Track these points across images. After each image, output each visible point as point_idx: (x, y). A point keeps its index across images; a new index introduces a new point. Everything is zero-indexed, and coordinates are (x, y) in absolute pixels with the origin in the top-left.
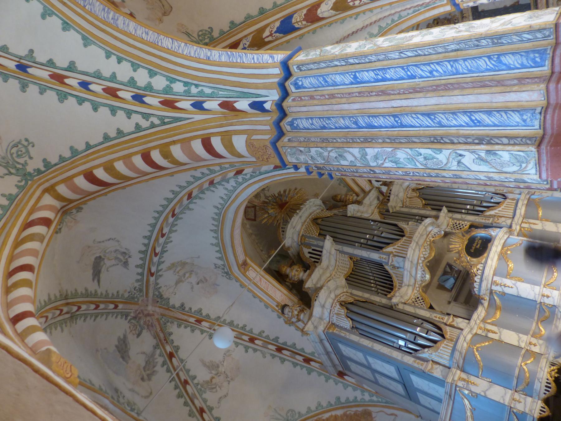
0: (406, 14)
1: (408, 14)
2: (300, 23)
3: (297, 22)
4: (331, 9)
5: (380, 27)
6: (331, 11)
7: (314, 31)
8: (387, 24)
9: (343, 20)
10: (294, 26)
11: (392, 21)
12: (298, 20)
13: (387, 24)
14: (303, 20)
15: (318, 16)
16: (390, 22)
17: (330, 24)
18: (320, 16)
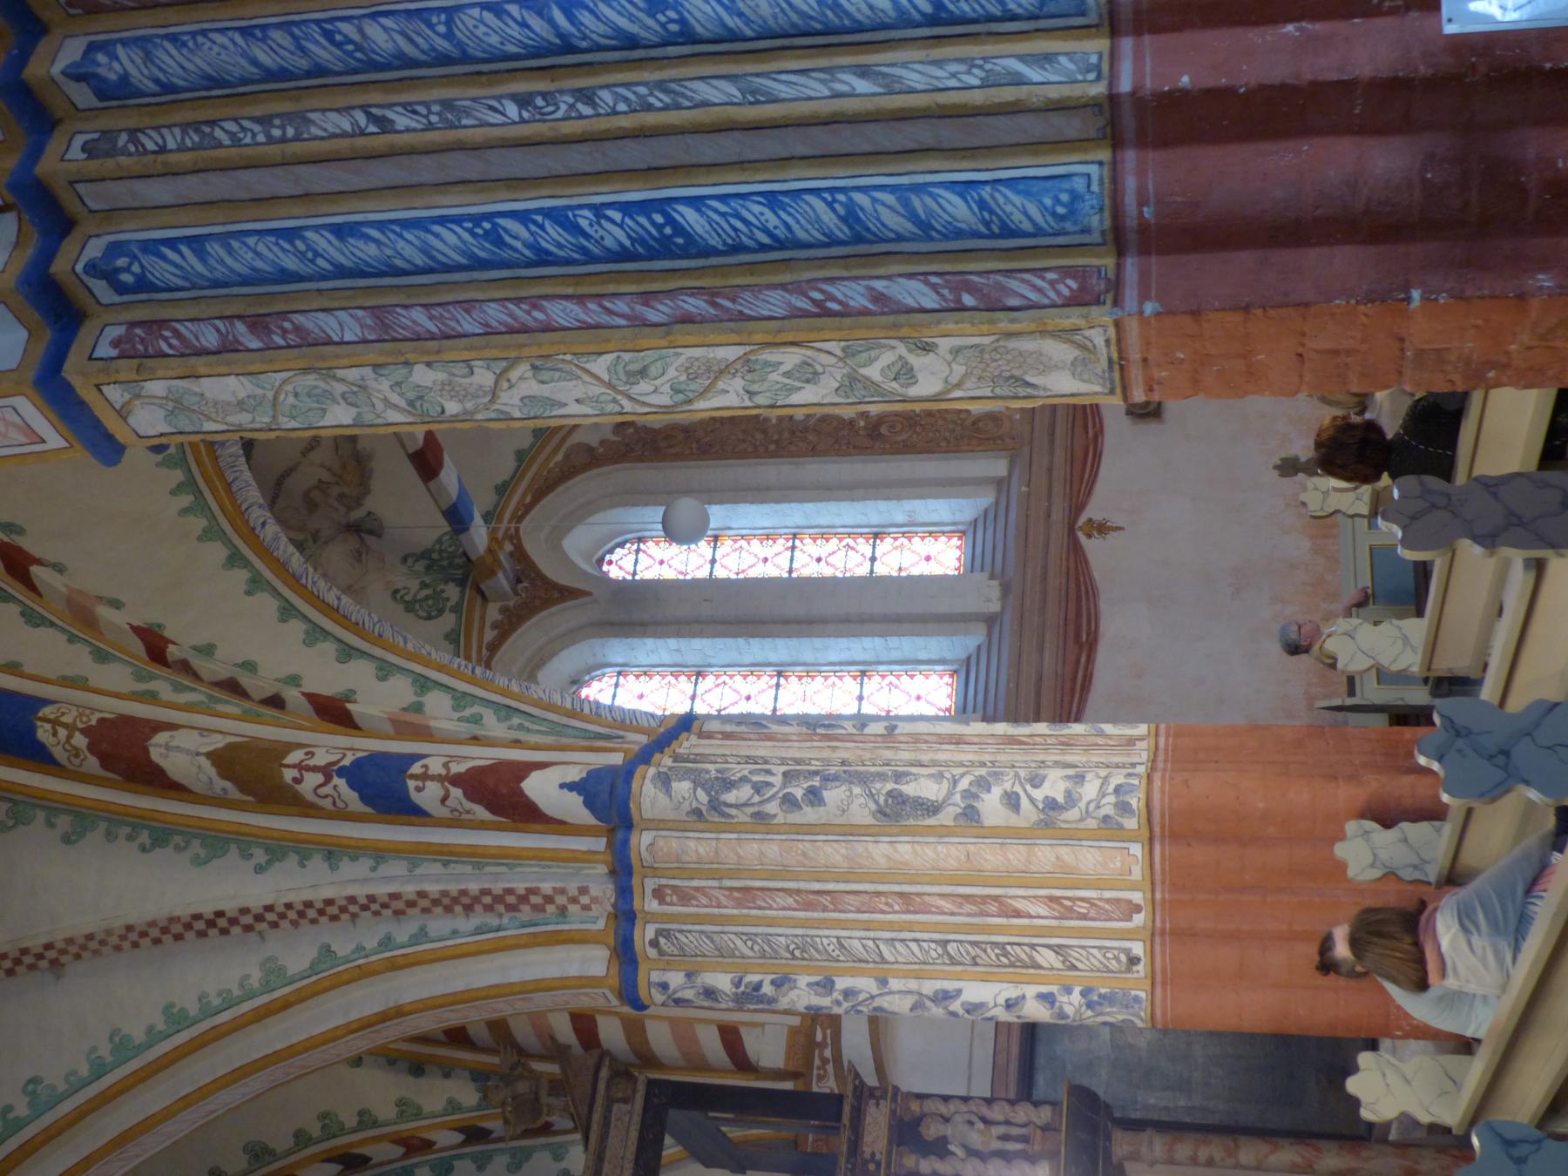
0: (446, 931)
1: (455, 933)
2: (62, 733)
3: (55, 723)
4: (209, 755)
5: (327, 950)
6: (206, 763)
7: (83, 818)
8: (360, 948)
9: (216, 842)
10: (33, 729)
11: (380, 944)
12: (66, 719)
13: (360, 948)
14: (83, 731)
15: (146, 751)
16: (371, 943)
17: (161, 834)
18: (156, 755)
